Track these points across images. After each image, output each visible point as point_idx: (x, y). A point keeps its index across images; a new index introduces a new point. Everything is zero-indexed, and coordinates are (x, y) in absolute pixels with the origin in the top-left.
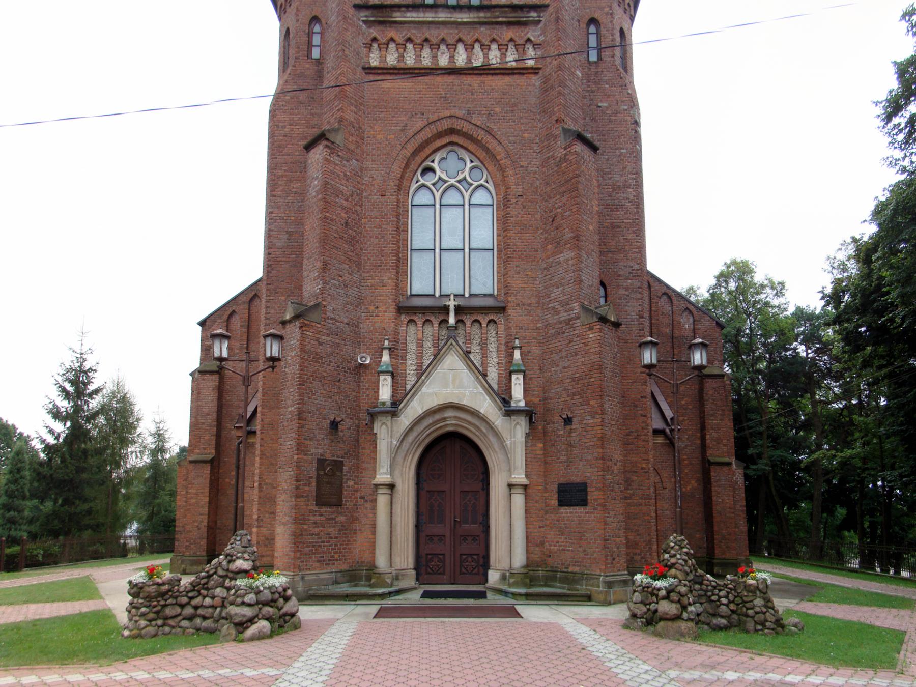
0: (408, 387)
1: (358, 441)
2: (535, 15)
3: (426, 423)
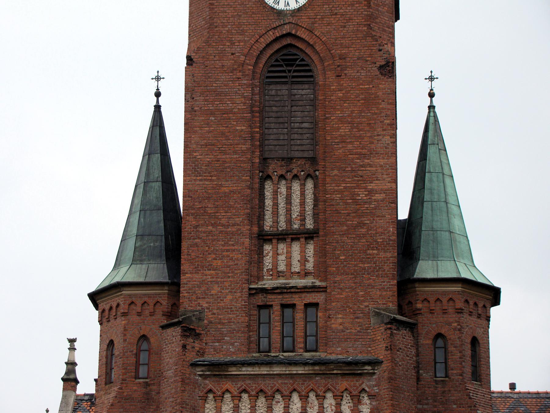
2: (370, 368)
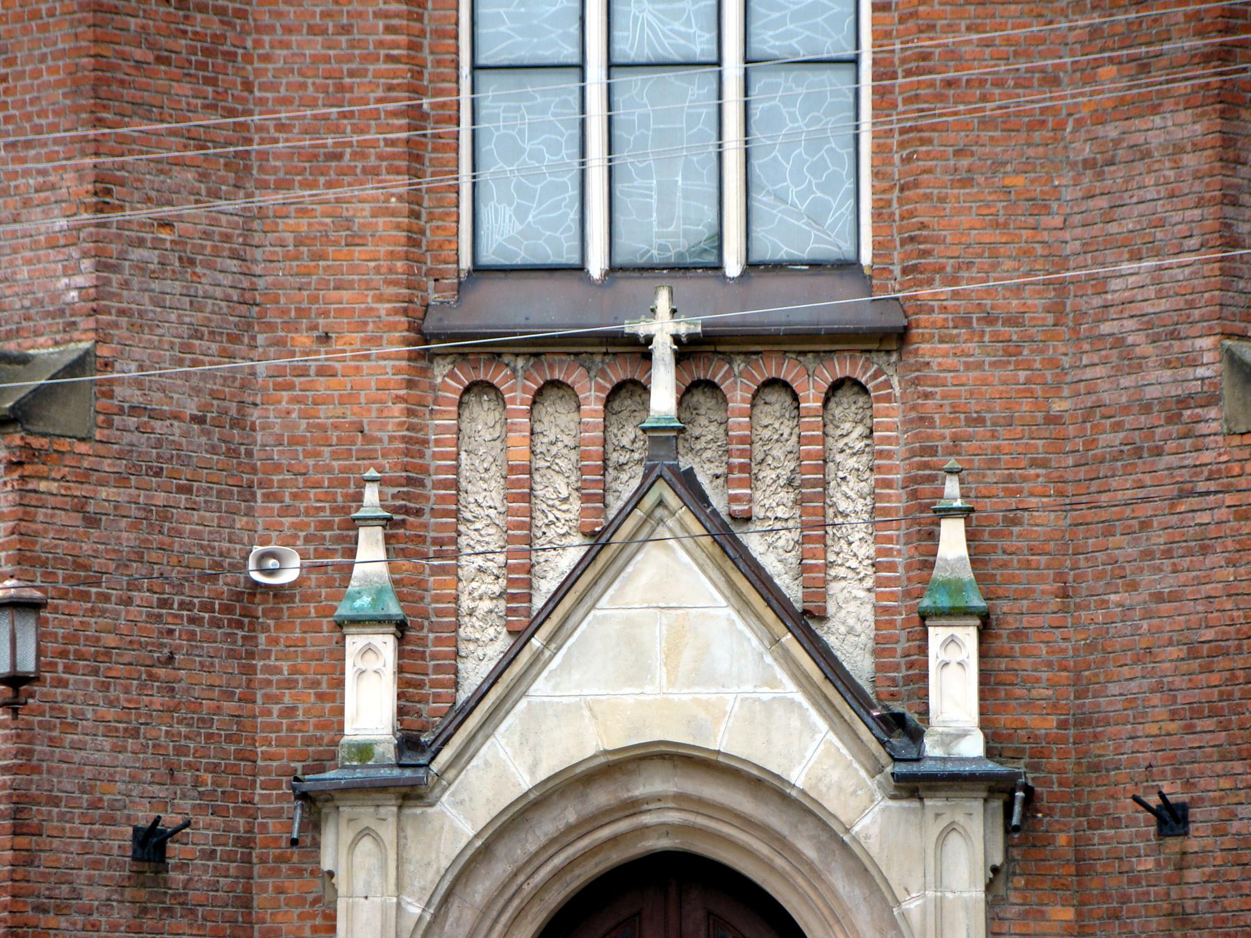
0: (473, 673)
1: (246, 903)
3: (547, 826)
